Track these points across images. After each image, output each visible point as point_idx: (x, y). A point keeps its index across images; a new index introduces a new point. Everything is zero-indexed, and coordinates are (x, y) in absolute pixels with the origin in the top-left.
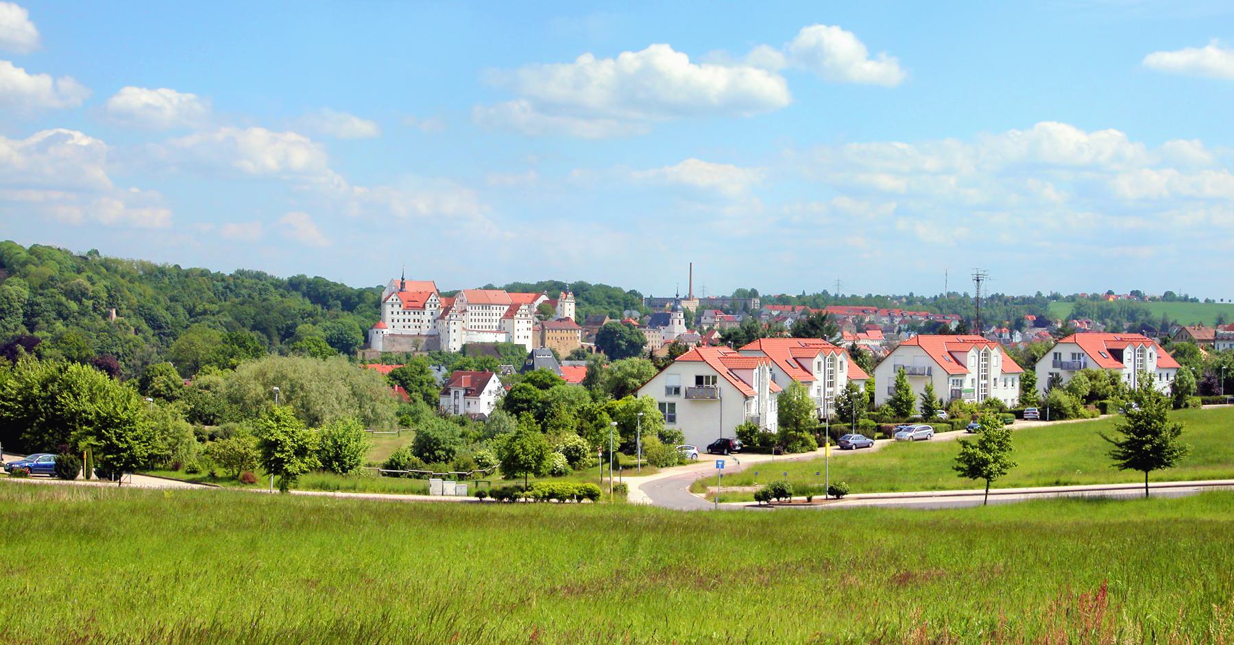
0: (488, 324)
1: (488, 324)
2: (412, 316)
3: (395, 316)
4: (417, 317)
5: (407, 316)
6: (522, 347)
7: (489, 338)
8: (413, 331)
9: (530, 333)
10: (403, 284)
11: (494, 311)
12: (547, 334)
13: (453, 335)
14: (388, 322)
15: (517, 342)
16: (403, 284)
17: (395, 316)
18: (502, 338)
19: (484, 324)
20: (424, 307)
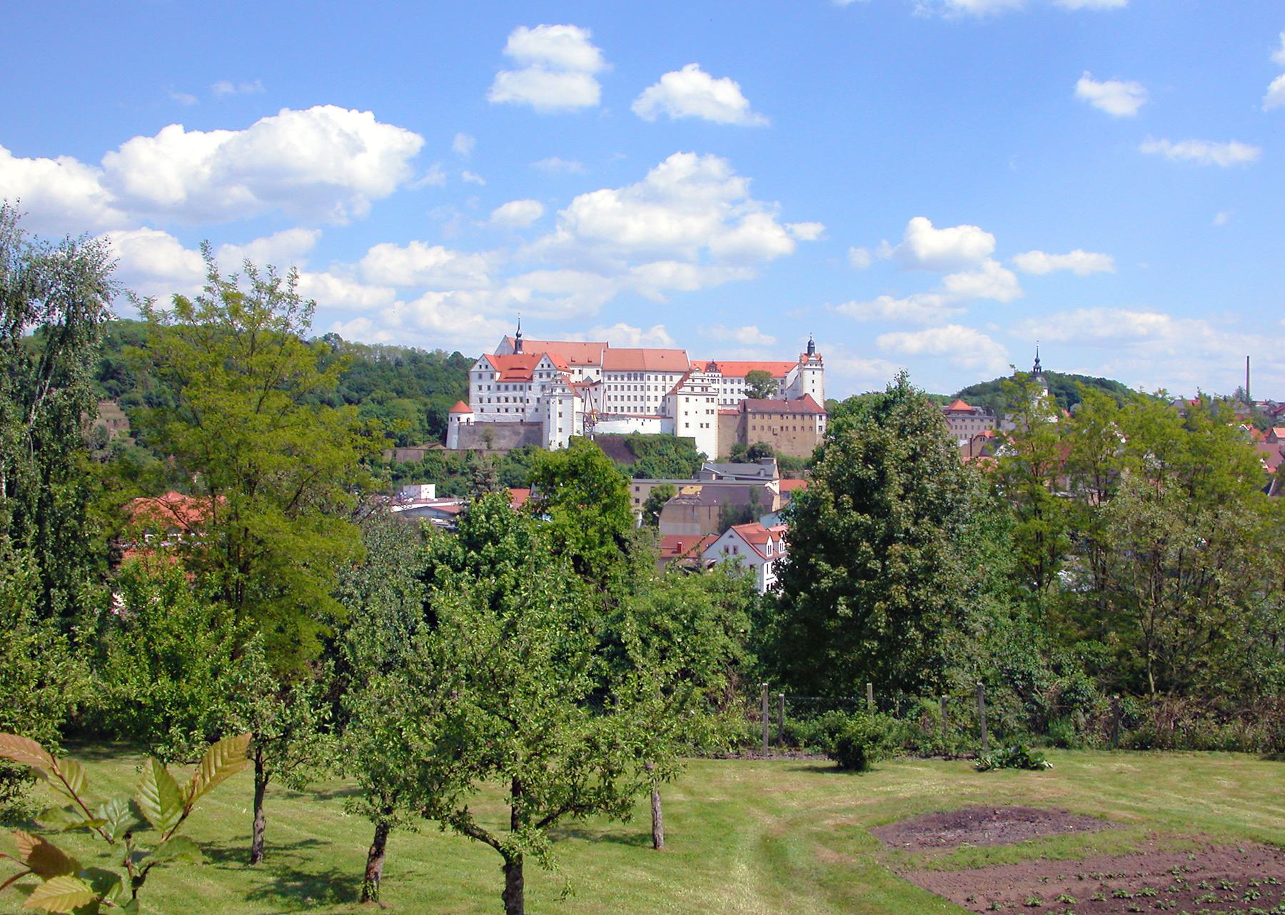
0: (639, 404)
1: (639, 404)
2: (511, 394)
3: (485, 393)
4: (519, 394)
5: (503, 394)
6: (690, 443)
7: (624, 428)
8: (513, 417)
9: (713, 420)
10: (518, 344)
11: (652, 383)
12: (751, 421)
13: (556, 423)
14: (474, 403)
15: (682, 432)
16: (518, 344)
17: (485, 393)
18: (654, 428)
19: (632, 404)
20: (531, 379)
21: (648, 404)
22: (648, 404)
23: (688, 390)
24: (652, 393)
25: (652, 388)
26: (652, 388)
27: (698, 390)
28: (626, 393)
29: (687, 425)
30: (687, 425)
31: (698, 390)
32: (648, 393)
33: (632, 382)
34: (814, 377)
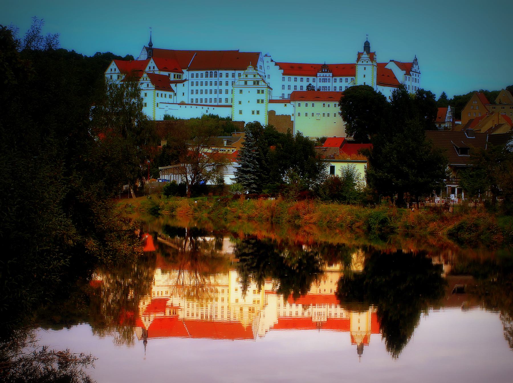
0: (213, 96)
1: (213, 96)
11: (224, 79)
21: (220, 96)
22: (220, 96)
23: (243, 83)
24: (223, 87)
25: (224, 83)
26: (224, 83)
27: (250, 83)
28: (204, 88)
29: (241, 112)
30: (241, 112)
31: (250, 83)
32: (220, 87)
33: (209, 80)
34: (365, 72)
